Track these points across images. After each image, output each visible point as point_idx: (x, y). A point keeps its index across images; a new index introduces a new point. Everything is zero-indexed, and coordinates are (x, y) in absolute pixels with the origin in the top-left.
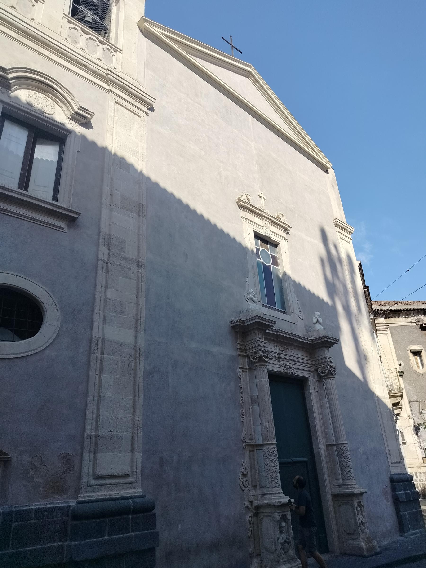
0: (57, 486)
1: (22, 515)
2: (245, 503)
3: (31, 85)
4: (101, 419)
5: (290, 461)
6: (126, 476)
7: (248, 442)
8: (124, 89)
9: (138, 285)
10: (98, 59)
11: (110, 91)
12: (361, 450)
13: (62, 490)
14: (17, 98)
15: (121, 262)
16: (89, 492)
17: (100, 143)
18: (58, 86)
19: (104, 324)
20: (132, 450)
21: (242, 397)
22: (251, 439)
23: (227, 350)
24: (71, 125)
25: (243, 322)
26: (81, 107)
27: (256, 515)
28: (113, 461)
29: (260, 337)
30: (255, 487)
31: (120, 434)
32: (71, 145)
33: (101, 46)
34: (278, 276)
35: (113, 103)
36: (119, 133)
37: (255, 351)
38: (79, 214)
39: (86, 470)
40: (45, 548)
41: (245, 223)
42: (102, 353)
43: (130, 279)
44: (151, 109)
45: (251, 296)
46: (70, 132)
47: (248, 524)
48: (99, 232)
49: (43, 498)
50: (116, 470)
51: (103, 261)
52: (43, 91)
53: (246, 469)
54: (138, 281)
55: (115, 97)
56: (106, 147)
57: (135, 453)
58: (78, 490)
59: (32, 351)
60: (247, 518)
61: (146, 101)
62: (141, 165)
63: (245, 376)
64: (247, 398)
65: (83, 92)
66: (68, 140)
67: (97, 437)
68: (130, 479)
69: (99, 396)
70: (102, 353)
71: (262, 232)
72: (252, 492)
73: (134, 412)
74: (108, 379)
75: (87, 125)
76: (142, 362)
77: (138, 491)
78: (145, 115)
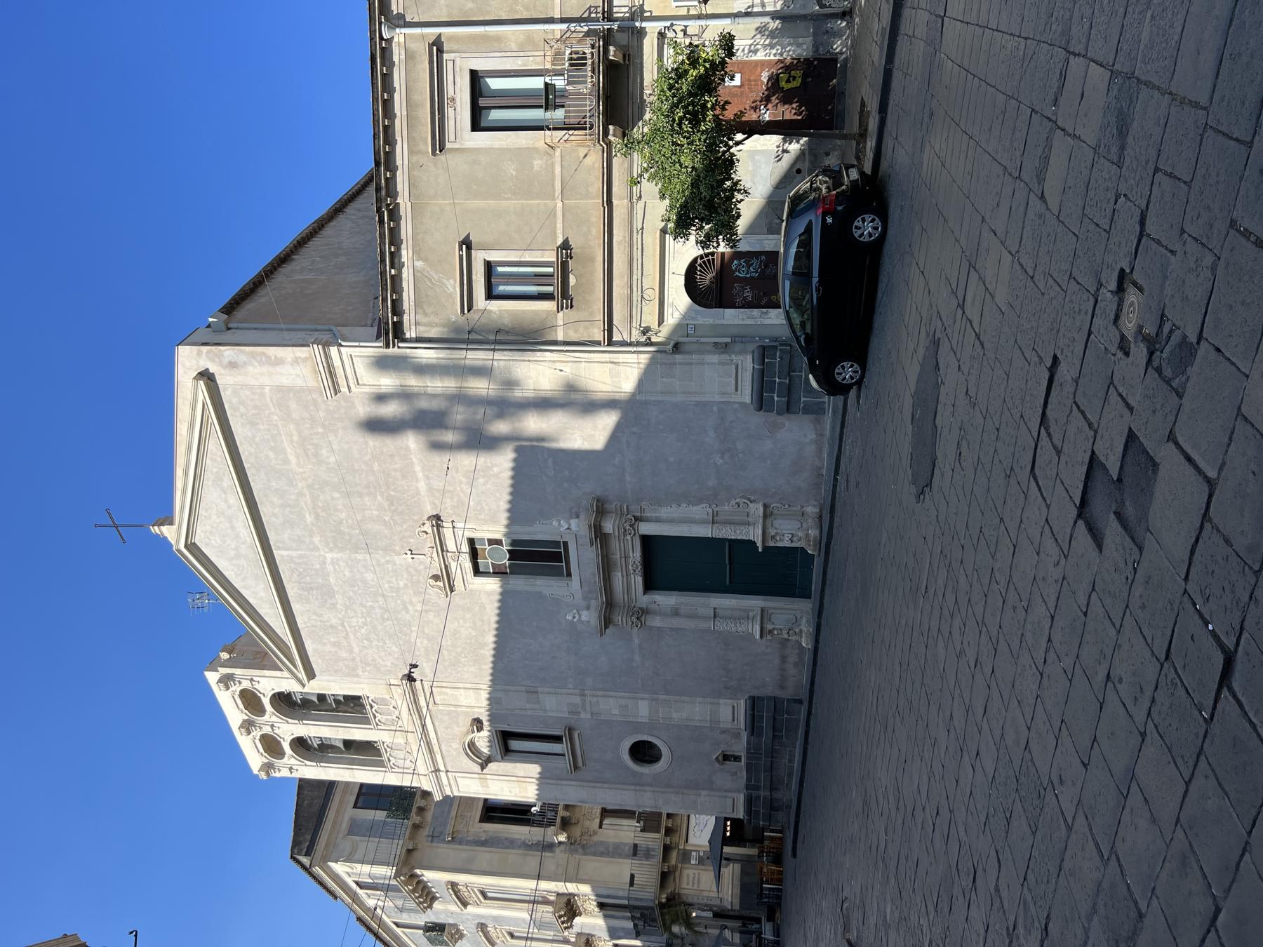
1: (748, 749)
8: (416, 701)
33: (375, 707)
41: (469, 587)
50: (730, 713)
77: (742, 702)
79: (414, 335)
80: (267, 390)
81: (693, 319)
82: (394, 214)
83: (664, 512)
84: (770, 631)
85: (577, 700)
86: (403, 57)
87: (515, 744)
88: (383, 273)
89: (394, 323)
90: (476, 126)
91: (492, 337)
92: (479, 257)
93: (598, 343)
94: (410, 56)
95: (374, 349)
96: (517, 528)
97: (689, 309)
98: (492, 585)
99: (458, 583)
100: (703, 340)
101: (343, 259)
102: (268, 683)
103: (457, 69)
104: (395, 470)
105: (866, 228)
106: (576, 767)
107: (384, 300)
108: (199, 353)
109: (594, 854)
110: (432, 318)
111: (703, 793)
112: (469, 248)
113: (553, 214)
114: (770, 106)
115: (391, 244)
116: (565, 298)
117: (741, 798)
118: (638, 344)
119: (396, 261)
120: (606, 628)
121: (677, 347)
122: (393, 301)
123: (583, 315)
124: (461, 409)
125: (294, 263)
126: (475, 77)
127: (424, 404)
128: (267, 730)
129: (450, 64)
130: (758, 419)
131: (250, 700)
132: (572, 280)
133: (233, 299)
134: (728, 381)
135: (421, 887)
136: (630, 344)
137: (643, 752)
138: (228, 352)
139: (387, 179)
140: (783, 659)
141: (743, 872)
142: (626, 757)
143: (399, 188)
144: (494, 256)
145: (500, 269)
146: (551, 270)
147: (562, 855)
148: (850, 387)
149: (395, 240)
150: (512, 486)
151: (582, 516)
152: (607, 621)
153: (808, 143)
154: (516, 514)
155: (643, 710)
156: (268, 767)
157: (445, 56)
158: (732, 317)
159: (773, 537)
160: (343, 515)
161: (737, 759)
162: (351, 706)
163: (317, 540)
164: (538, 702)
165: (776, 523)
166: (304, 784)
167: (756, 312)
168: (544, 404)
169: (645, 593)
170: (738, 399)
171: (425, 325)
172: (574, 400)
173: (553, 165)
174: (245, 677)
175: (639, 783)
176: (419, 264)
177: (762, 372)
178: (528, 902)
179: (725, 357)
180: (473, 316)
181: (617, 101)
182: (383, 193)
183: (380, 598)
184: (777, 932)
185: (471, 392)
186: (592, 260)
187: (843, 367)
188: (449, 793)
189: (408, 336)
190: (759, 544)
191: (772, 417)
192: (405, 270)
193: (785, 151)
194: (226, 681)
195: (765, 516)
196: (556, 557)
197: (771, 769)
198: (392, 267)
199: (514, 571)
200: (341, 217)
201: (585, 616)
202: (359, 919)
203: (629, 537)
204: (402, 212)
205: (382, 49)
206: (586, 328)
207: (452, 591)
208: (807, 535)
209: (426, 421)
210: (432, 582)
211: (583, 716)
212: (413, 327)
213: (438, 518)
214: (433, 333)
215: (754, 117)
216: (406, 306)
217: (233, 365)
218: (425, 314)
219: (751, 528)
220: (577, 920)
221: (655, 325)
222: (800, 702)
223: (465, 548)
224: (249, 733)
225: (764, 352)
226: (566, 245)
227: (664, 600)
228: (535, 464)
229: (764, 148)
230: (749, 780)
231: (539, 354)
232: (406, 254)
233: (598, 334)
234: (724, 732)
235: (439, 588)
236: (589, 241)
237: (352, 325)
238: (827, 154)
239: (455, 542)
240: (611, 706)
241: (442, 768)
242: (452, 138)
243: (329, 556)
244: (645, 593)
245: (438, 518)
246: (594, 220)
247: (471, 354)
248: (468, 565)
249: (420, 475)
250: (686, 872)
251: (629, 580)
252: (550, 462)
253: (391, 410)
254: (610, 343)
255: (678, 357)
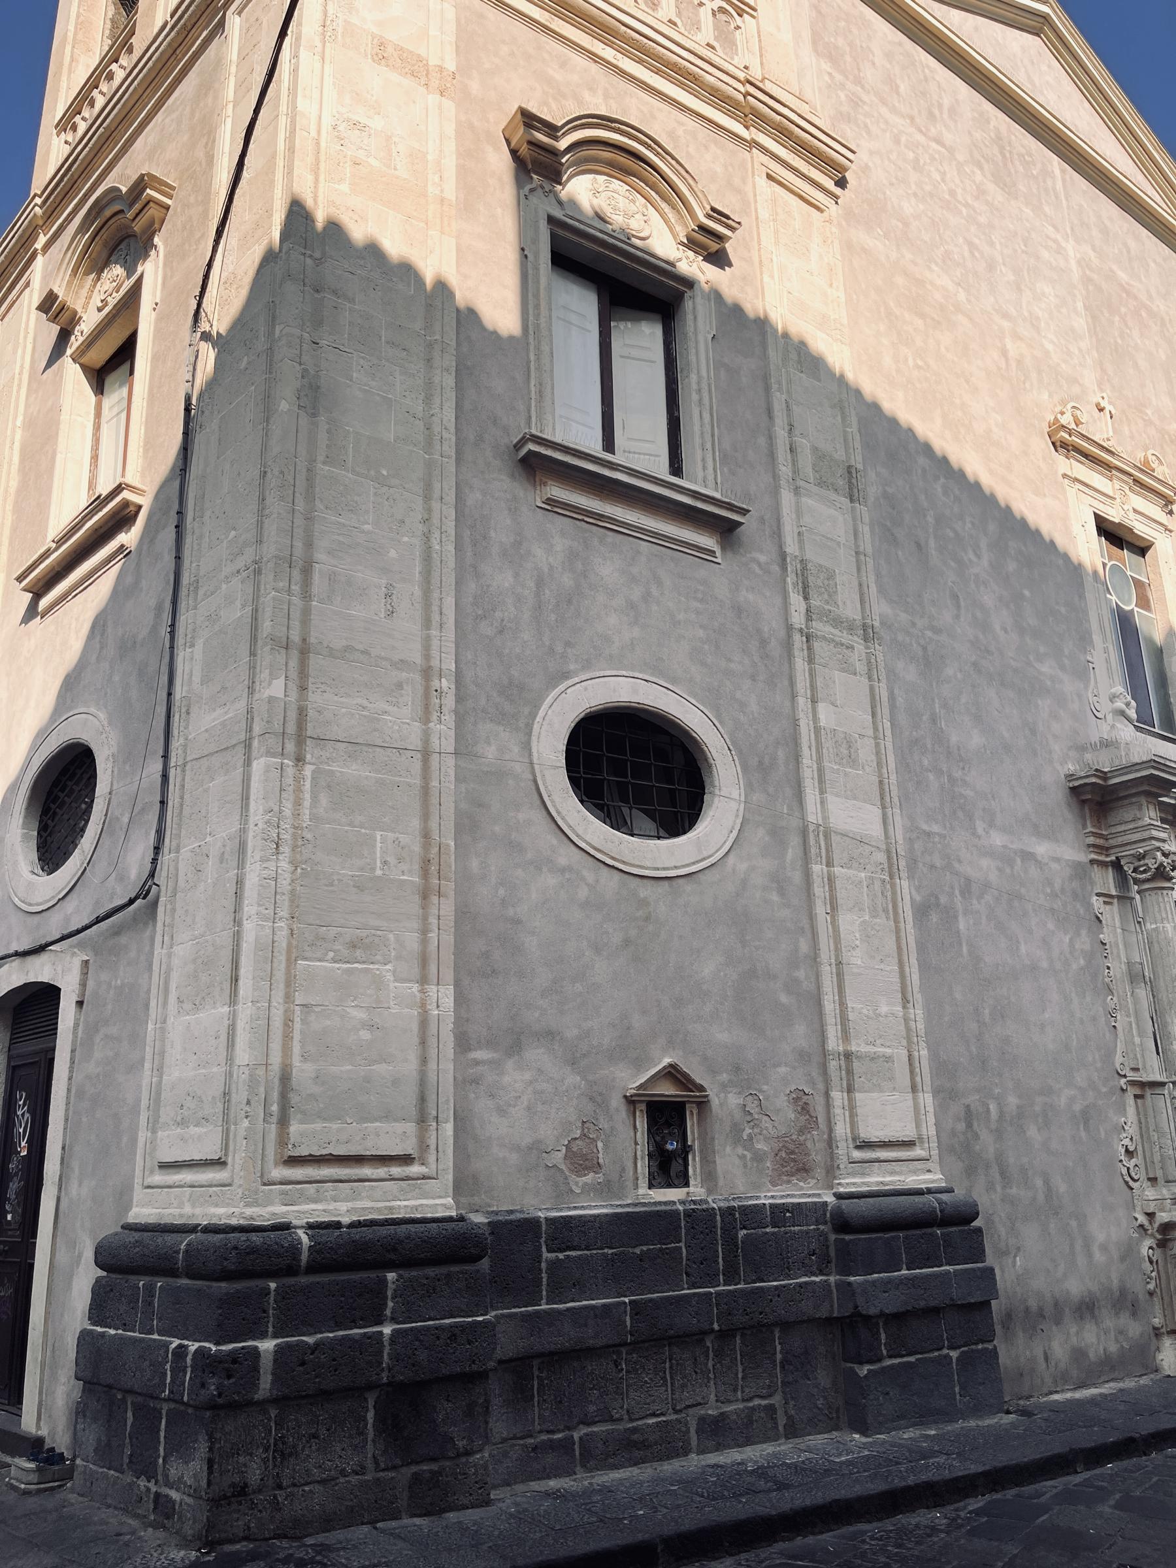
0: (793, 1163)
1: (751, 1215)
2: (1137, 1215)
3: (596, 160)
4: (851, 1016)
6: (909, 1144)
7: (1133, 1076)
8: (783, 133)
9: (872, 688)
10: (708, 45)
11: (754, 144)
13: (804, 1170)
14: (573, 203)
15: (833, 630)
16: (853, 1174)
17: (753, 306)
18: (657, 154)
19: (822, 792)
20: (914, 1089)
21: (1108, 968)
22: (1136, 1070)
23: (1063, 848)
24: (690, 265)
25: (1104, 776)
26: (713, 209)
27: (1162, 1244)
28: (887, 1111)
29: (1150, 815)
30: (1153, 1180)
31: (888, 1051)
32: (698, 322)
34: (1150, 642)
35: (762, 181)
36: (791, 273)
37: (1141, 851)
38: (744, 512)
39: (841, 1129)
40: (800, 1285)
42: (829, 864)
43: (855, 674)
44: (842, 183)
45: (1120, 704)
46: (689, 283)
47: (1147, 1267)
48: (783, 556)
49: (774, 1184)
51: (801, 630)
52: (623, 172)
53: (1131, 1139)
54: (870, 678)
55: (765, 159)
56: (766, 317)
57: (921, 1094)
58: (831, 1170)
59: (704, 859)
60: (1145, 1251)
61: (832, 160)
62: (838, 355)
63: (1111, 915)
64: (1118, 969)
65: (717, 166)
66: (688, 304)
67: (848, 1056)
68: (918, 1152)
69: (839, 963)
70: (829, 864)
71: (1114, 515)
72: (1150, 1193)
73: (905, 1001)
74: (849, 922)
75: (719, 259)
76: (905, 884)
77: (932, 1178)
111: (443, 998)
117: (434, 1201)
140: (1086, 1308)
161: (668, 1166)
197: (660, 1339)
230: (565, 1231)
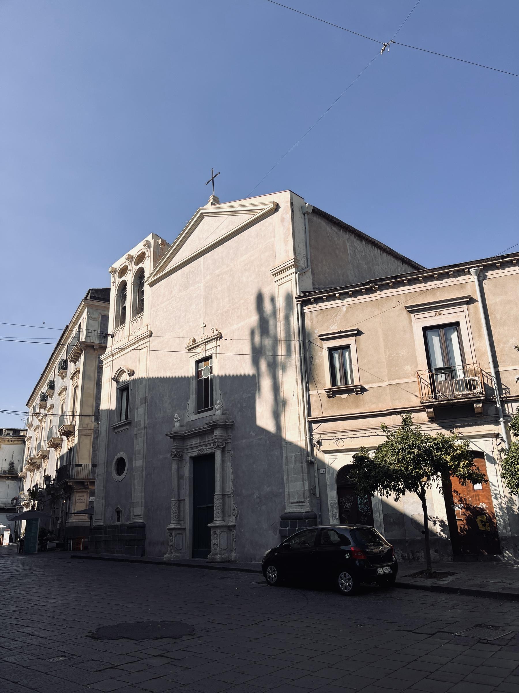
5: (205, 506)
6: (140, 515)
12: (256, 495)
33: (139, 319)
50: (137, 514)
74: (136, 482)
77: (142, 520)
78: (148, 343)
79: (305, 311)
80: (273, 239)
81: (329, 471)
82: (369, 291)
83: (228, 465)
84: (171, 534)
85: (142, 425)
86: (461, 282)
87: (125, 394)
88: (336, 290)
89: (310, 299)
90: (425, 329)
91: (308, 354)
92: (351, 341)
93: (309, 414)
94: (462, 286)
95: (295, 292)
96: (218, 381)
97: (334, 470)
98: (191, 372)
99: (191, 354)
100: (317, 479)
101: (365, 266)
102: (148, 265)
103: (458, 314)
104: (241, 312)
105: (345, 582)
106: (114, 429)
107: (321, 293)
108: (287, 202)
109: (94, 444)
110: (315, 320)
112: (356, 335)
113: (381, 380)
114: (464, 510)
115: (353, 291)
116: (333, 393)
117: (101, 523)
118: (311, 440)
119: (345, 296)
120: (171, 437)
121: (311, 464)
122: (322, 297)
123: (325, 404)
124: (270, 342)
125: (358, 242)
126: (456, 325)
127: (271, 322)
128: (129, 268)
129: (461, 309)
130: (277, 518)
131: (141, 258)
132: (344, 396)
133: (326, 214)
134: (295, 496)
135: (78, 355)
136: (311, 435)
137: (121, 465)
138: (288, 216)
139: (388, 284)
141: (85, 527)
142: (119, 456)
143: (384, 292)
144: (353, 348)
145: (347, 354)
146: (350, 383)
147: (93, 426)
148: (265, 575)
149: (355, 294)
150: (237, 375)
151: (223, 417)
152: (175, 437)
153: (441, 538)
154: (224, 379)
155: (138, 463)
156: (114, 271)
157: (465, 306)
158: (332, 496)
159: (215, 533)
160: (220, 289)
161: (118, 520)
162: (139, 307)
163: (208, 277)
164: (141, 404)
165: (225, 534)
166: (108, 290)
167: (336, 511)
168: (276, 388)
169: (191, 457)
170: (287, 504)
171: (311, 317)
172: (279, 406)
173: (409, 377)
174: (150, 253)
175: (108, 464)
176: (344, 308)
177: (300, 518)
178: (73, 412)
179: (307, 494)
180: (318, 342)
181: (447, 413)
182: (380, 283)
183: (184, 314)
184: (51, 550)
185: (279, 347)
186: (357, 406)
187: (274, 571)
188: (104, 363)
189: (304, 308)
190: (212, 524)
191: (279, 527)
192: (340, 301)
193: (435, 523)
194: (148, 245)
195: (229, 527)
196: (206, 405)
198: (341, 294)
199: (199, 382)
200: (399, 263)
201: (177, 424)
202: (67, 327)
203: (212, 445)
204: (372, 295)
205: (463, 270)
206: (318, 407)
207: (189, 350)
208: (217, 554)
209: (264, 325)
210: (191, 339)
211: (135, 429)
212: (309, 310)
213: (221, 337)
214: (307, 322)
215: (456, 500)
216: (320, 304)
217: (283, 220)
218: (317, 316)
219: (220, 519)
220: (65, 438)
221: (323, 448)
222: (143, 555)
223: (207, 355)
224: (127, 259)
225: (312, 518)
226: (363, 390)
227: (187, 469)
228: (248, 386)
229: (435, 509)
231: (300, 381)
232: (349, 301)
233: (315, 414)
234: (130, 511)
235: (189, 343)
236: (367, 403)
237: (313, 278)
238: (436, 551)
239: (210, 349)
240: (139, 445)
241: (114, 358)
242: (417, 317)
243: (202, 285)
244: (191, 457)
245: (221, 337)
246: (380, 405)
247: (297, 343)
248: (200, 357)
249: (240, 325)
250: (85, 495)
251: (195, 448)
252: (249, 395)
253: (268, 306)
254: (310, 423)
255: (305, 465)
